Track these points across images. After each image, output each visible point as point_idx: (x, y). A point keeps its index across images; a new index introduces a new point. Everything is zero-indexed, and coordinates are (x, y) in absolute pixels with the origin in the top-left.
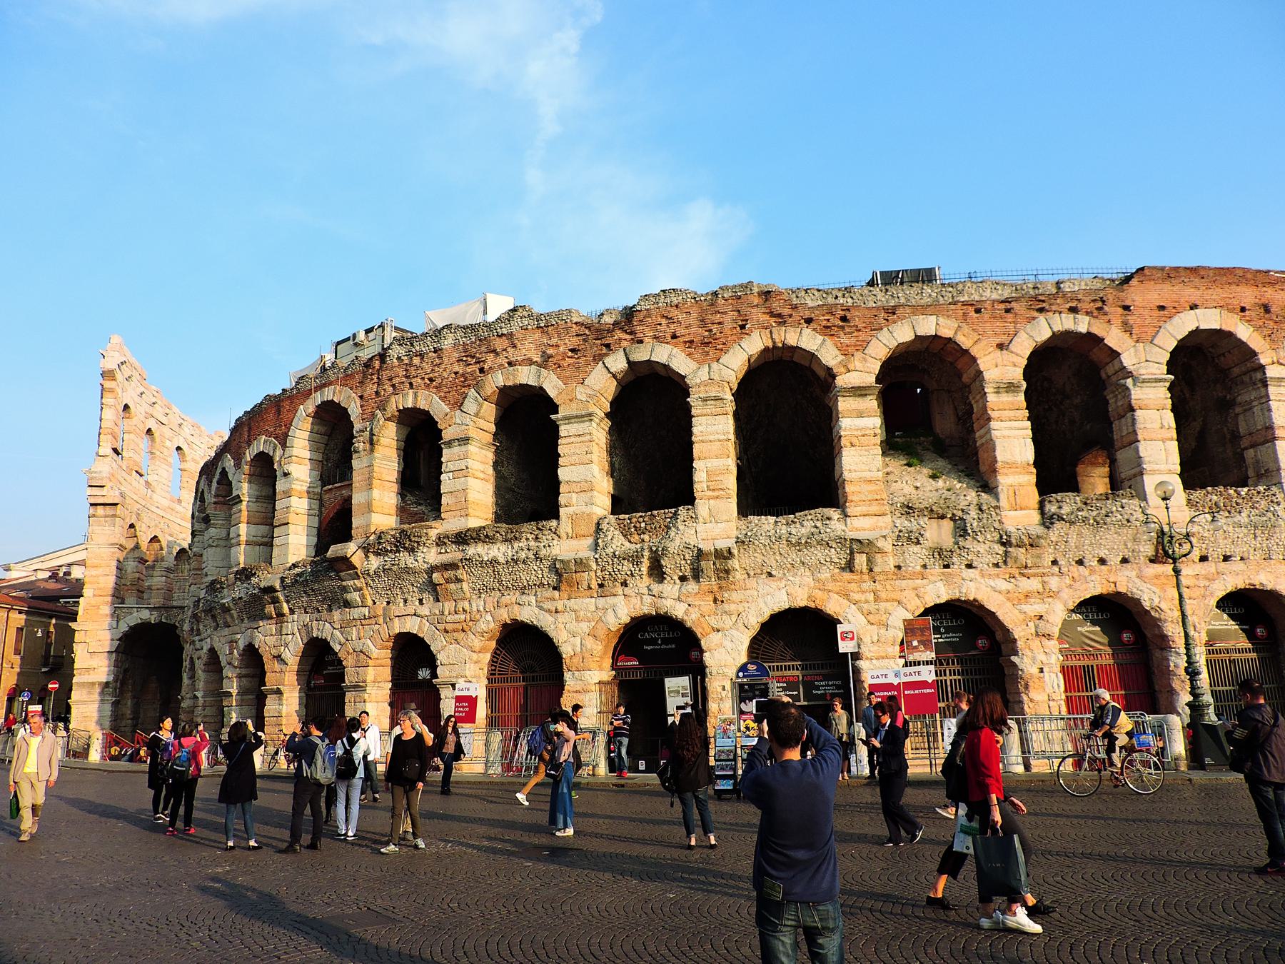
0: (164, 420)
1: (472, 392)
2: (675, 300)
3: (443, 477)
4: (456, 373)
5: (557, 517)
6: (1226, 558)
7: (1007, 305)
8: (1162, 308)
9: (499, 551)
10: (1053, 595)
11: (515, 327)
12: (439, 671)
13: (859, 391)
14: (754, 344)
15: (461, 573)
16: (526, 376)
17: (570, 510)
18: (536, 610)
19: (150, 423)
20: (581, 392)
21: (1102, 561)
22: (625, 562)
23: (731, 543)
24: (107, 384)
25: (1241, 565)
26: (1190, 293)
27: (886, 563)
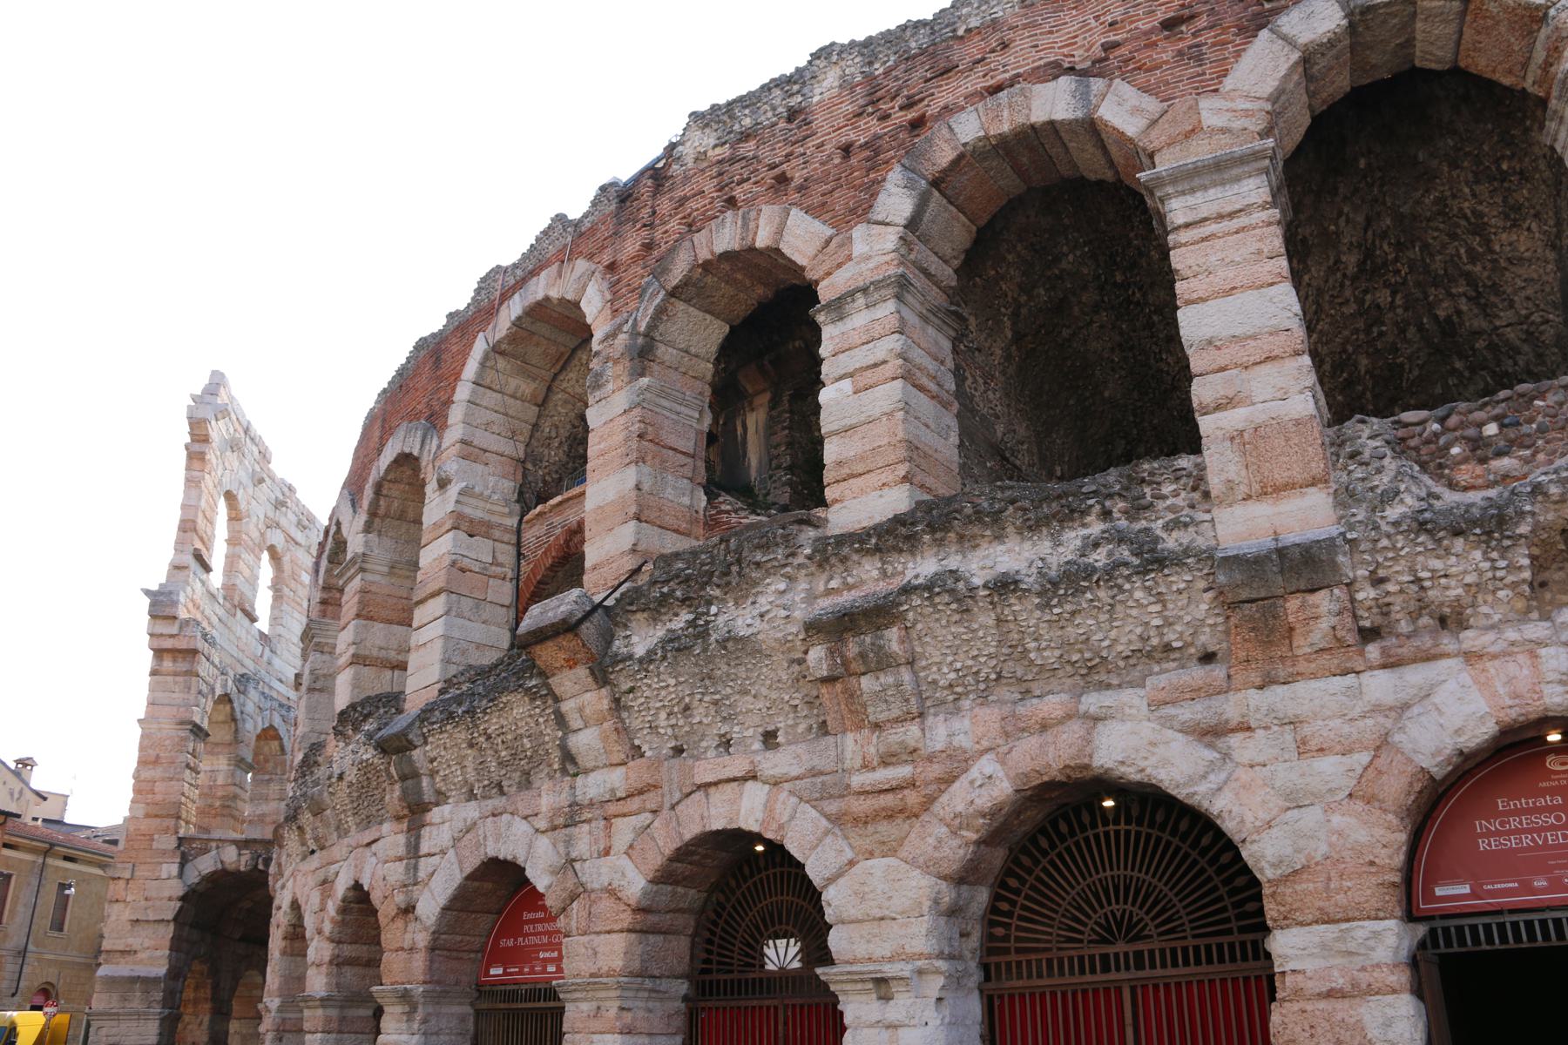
0: (299, 536)
1: (895, 176)
3: (825, 396)
4: (847, 150)
12: (836, 941)
15: (893, 635)
16: (1053, 103)
17: (1234, 418)
18: (1148, 729)
19: (276, 538)
20: (1211, 112)
22: (1459, 544)
24: (197, 447)
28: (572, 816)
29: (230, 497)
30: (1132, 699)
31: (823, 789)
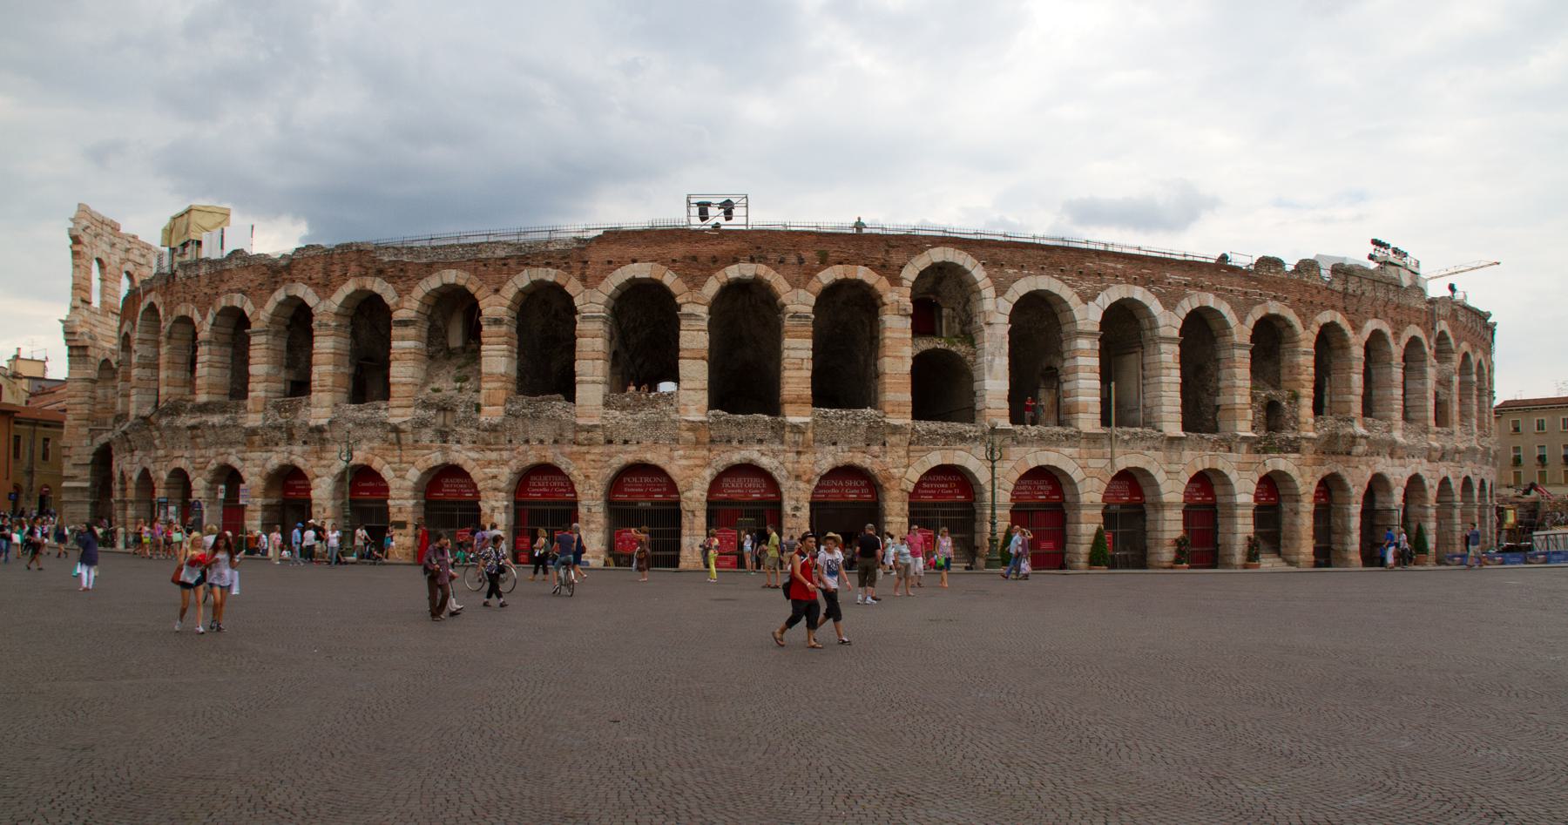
0: (142, 261)
2: (312, 253)
5: (246, 397)
6: (626, 442)
7: (504, 261)
8: (610, 262)
9: (216, 419)
10: (506, 463)
11: (232, 265)
13: (404, 323)
14: (349, 287)
16: (237, 300)
21: (541, 442)
23: (323, 422)
24: (77, 248)
25: (635, 448)
26: (634, 251)
27: (408, 438)
28: (156, 460)
29: (99, 261)
30: (233, 451)
31: (192, 459)
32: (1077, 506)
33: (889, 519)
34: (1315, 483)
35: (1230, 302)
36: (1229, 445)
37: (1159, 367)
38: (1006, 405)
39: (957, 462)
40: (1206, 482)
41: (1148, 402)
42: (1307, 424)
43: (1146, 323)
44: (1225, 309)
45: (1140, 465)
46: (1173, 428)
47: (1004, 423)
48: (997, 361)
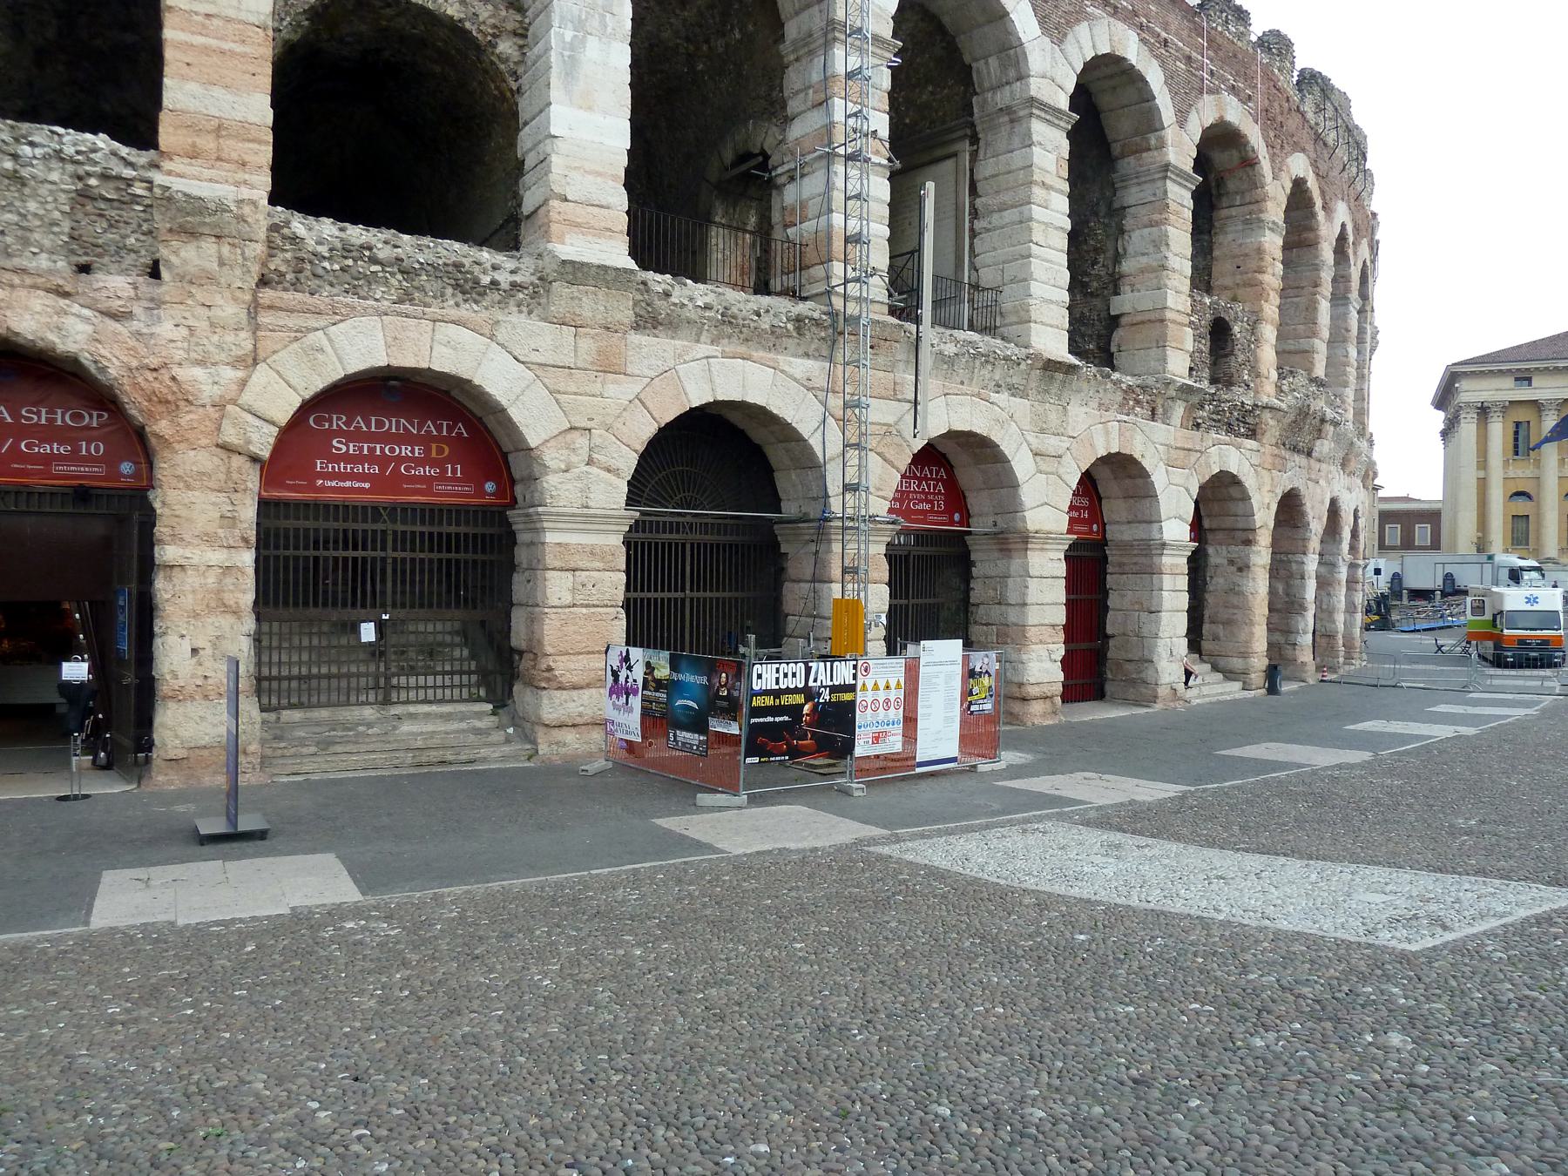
32: (820, 526)
33: (167, 553)
34: (1274, 507)
35: (1163, 65)
36: (1150, 401)
37: (1025, 177)
38: (620, 199)
39: (443, 362)
40: (1108, 486)
41: (987, 277)
42: (1265, 381)
43: (988, 69)
44: (1155, 77)
45: (980, 427)
46: (1051, 339)
47: (617, 254)
48: (593, 49)
